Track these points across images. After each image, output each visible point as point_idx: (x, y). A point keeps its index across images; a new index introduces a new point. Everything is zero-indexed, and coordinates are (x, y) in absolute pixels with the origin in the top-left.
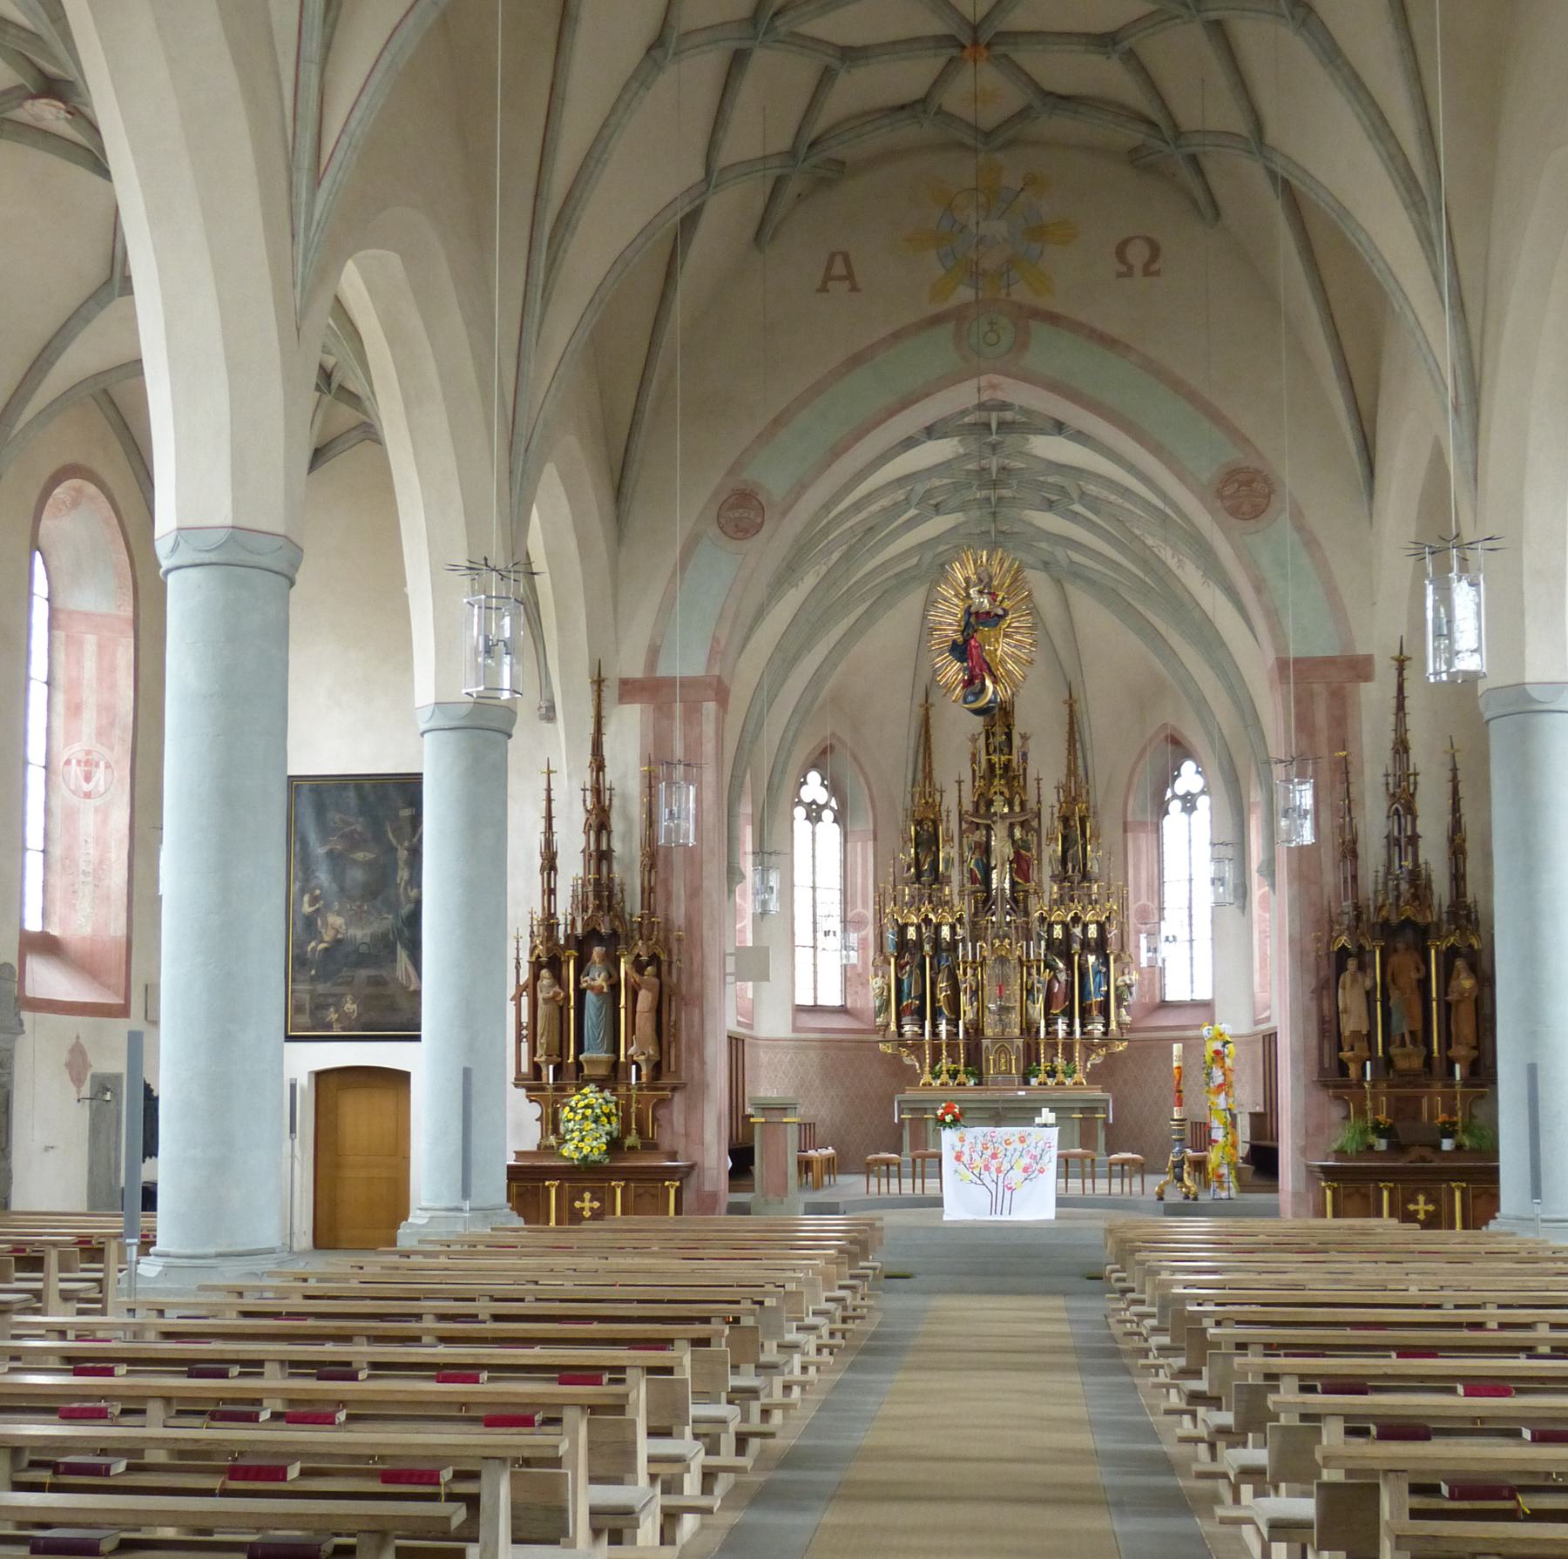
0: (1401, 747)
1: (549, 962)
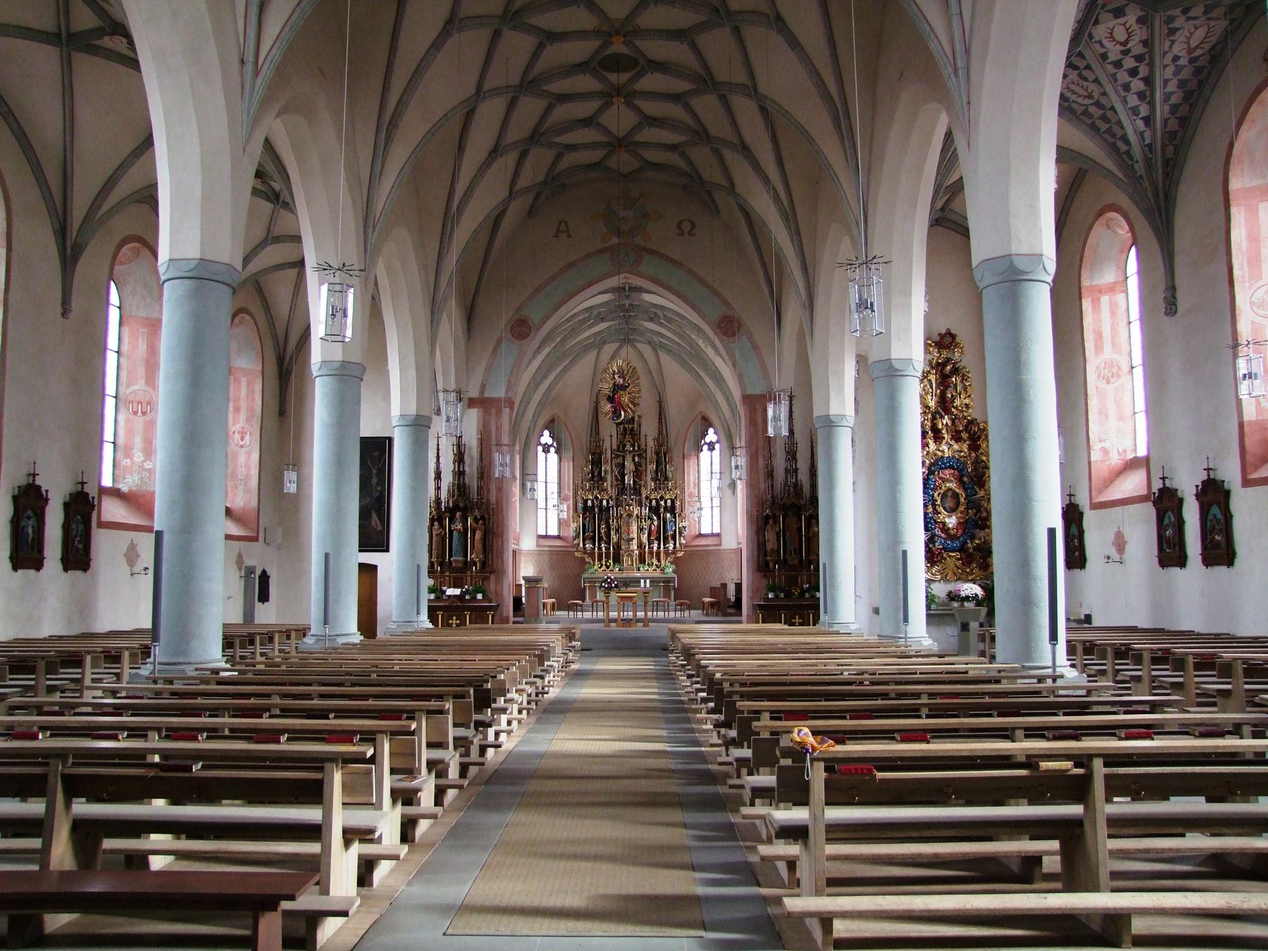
1: (437, 518)
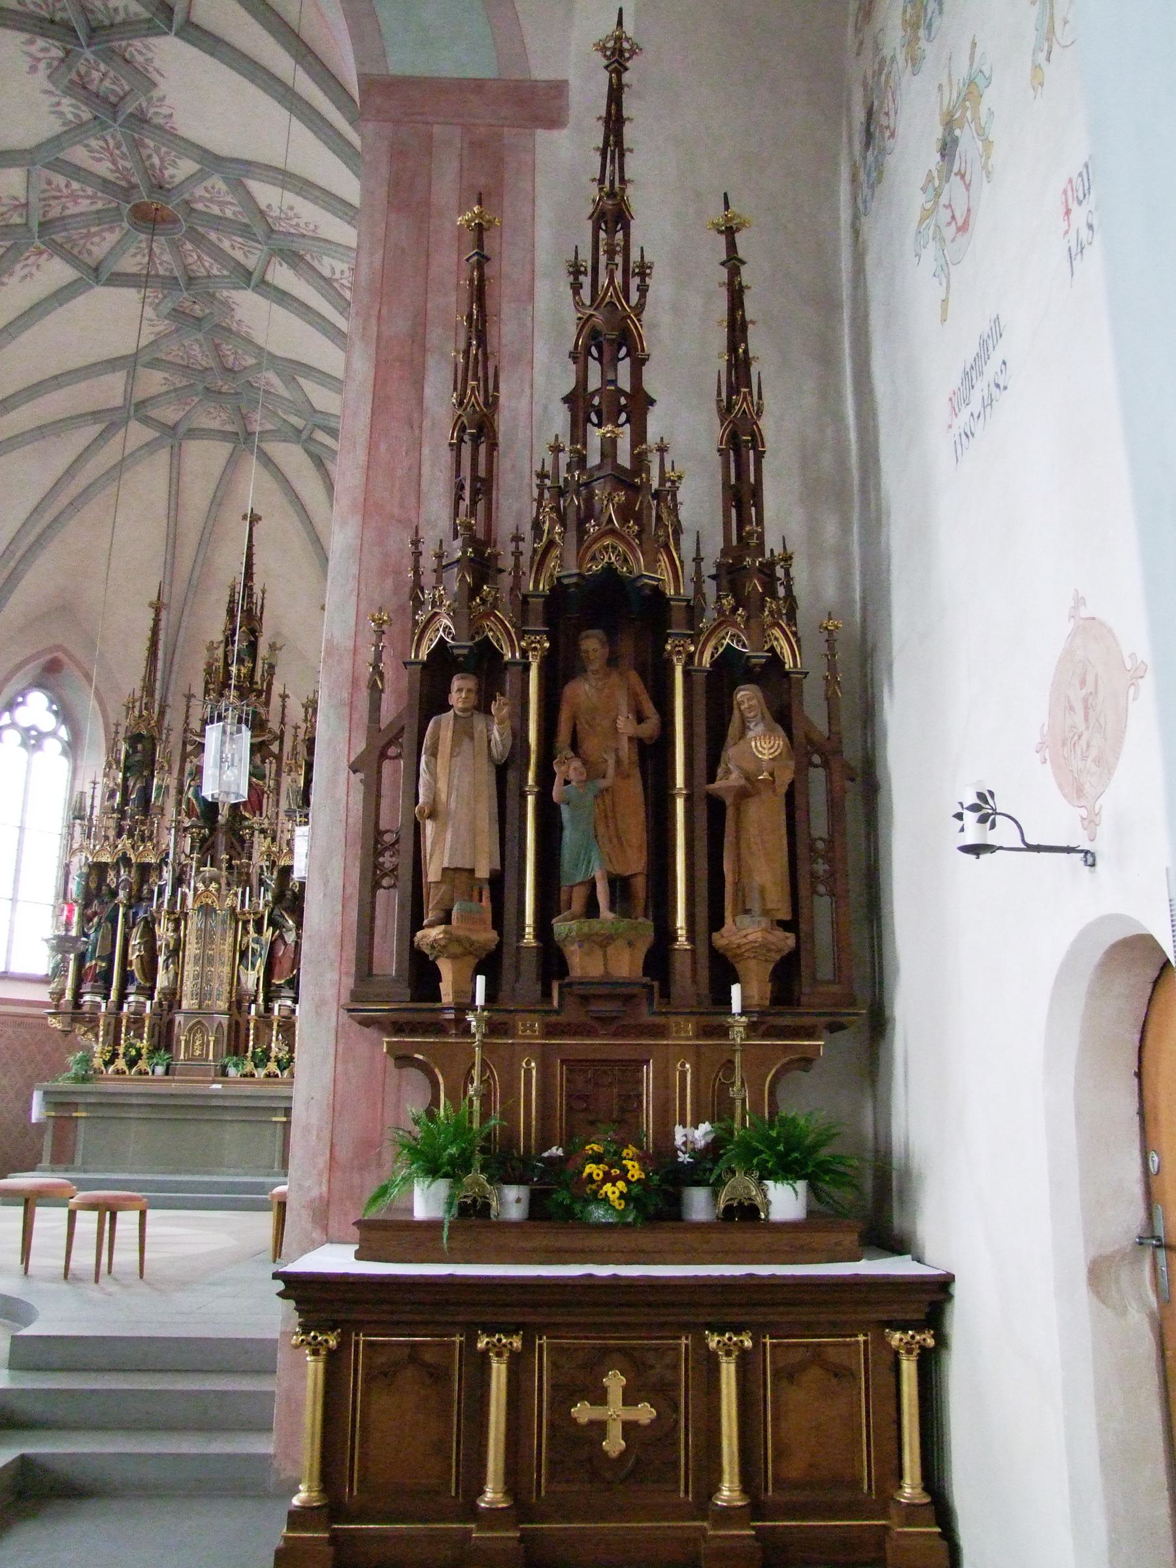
0: (612, 215)
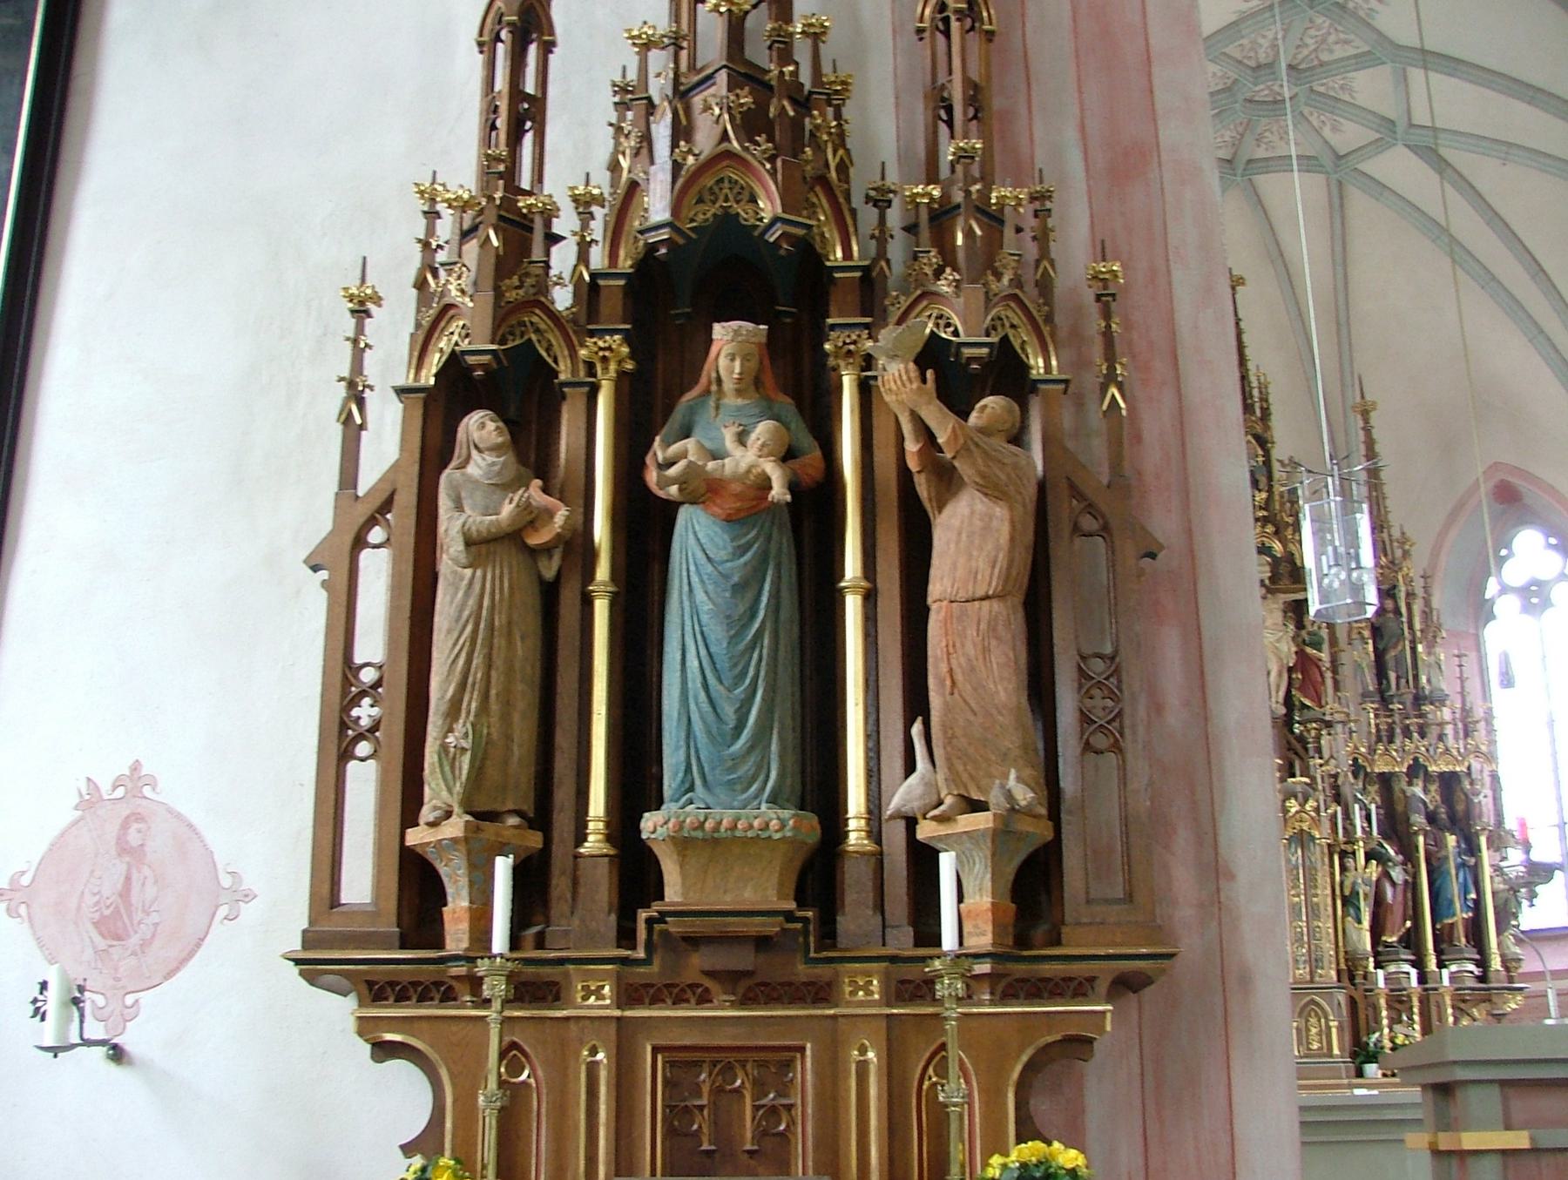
1: (494, 385)
